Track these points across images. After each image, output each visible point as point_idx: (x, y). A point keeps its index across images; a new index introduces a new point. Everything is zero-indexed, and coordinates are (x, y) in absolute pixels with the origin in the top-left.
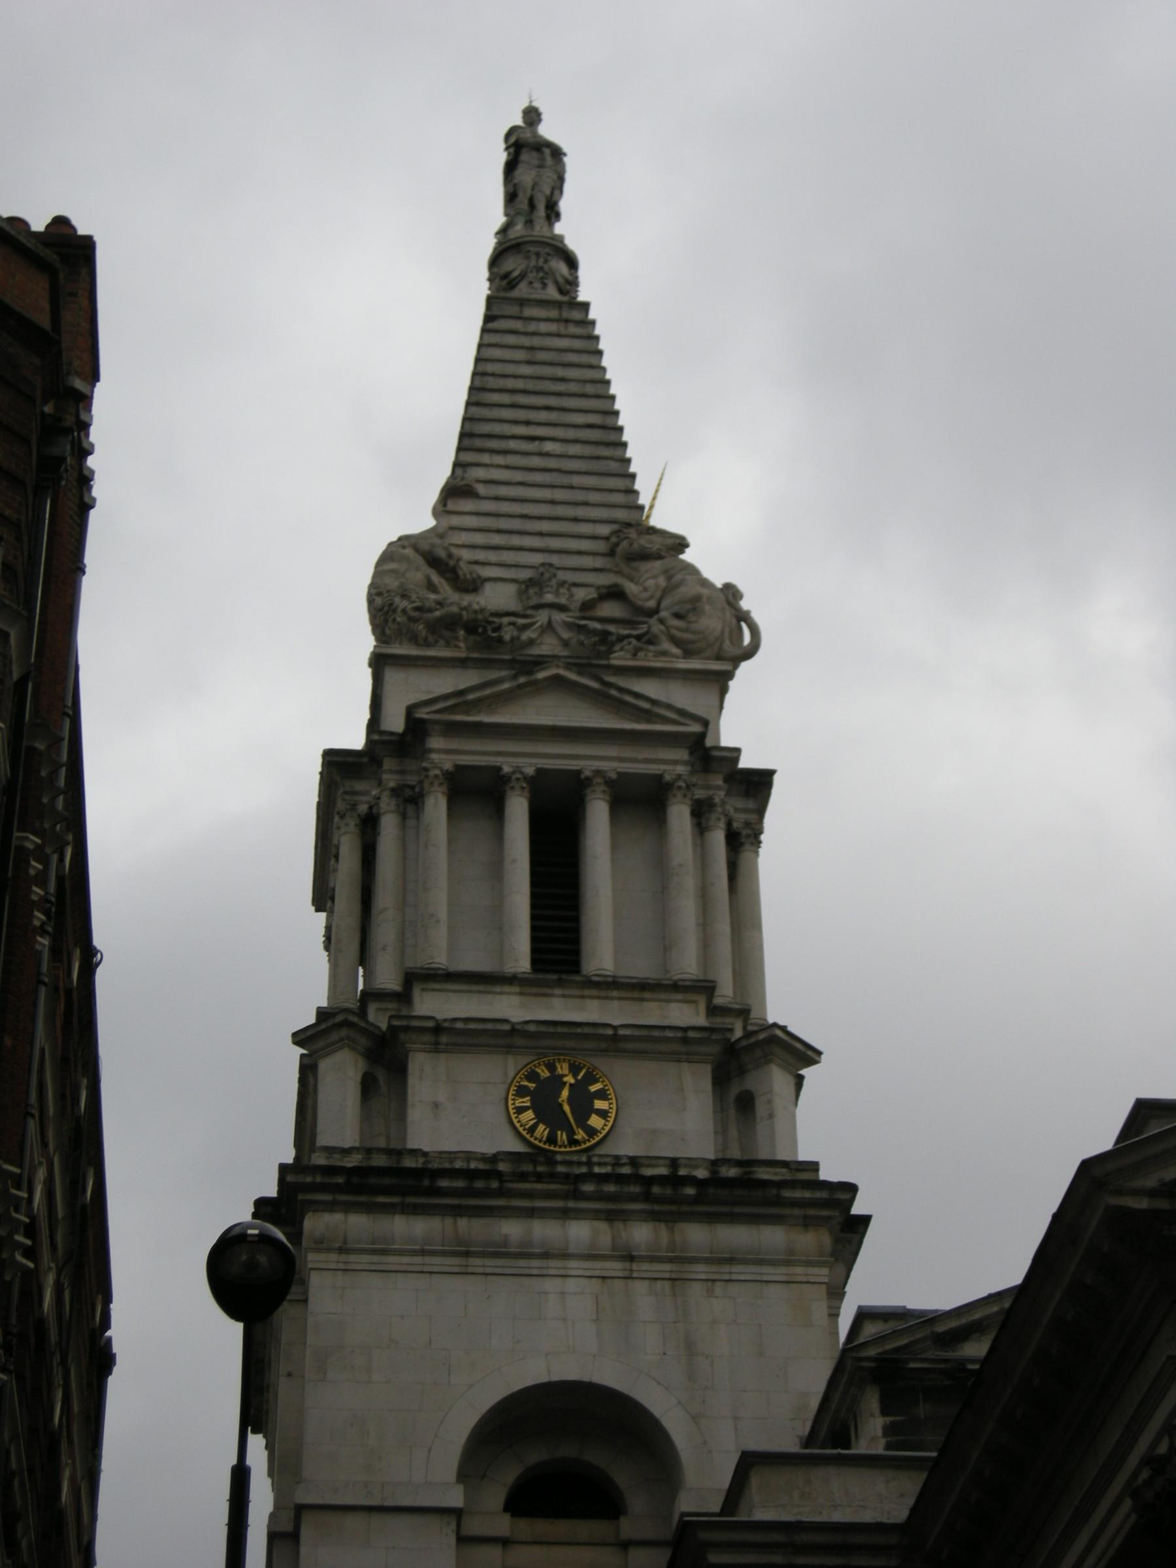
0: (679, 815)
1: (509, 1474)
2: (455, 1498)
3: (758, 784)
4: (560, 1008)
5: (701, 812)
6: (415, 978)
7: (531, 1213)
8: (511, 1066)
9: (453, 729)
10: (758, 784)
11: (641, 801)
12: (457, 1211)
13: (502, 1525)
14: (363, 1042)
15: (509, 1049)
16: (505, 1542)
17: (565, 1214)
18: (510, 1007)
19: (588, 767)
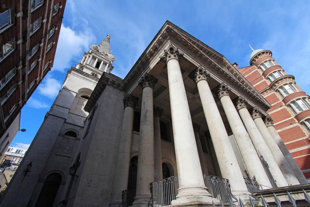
0: (108, 65)
1: (82, 94)
2: (77, 92)
3: (113, 67)
4: (96, 70)
5: (109, 66)
6: (86, 64)
7: (90, 78)
8: (92, 72)
9: (94, 53)
10: (113, 67)
11: (105, 64)
12: (84, 76)
13: (80, 97)
14: (81, 66)
15: (92, 71)
16: (80, 98)
17: (93, 79)
18: (93, 69)
19: (102, 59)
